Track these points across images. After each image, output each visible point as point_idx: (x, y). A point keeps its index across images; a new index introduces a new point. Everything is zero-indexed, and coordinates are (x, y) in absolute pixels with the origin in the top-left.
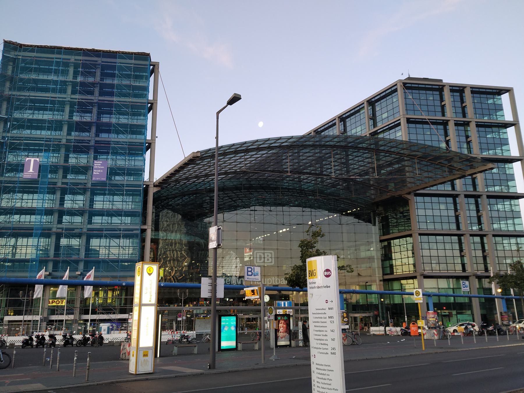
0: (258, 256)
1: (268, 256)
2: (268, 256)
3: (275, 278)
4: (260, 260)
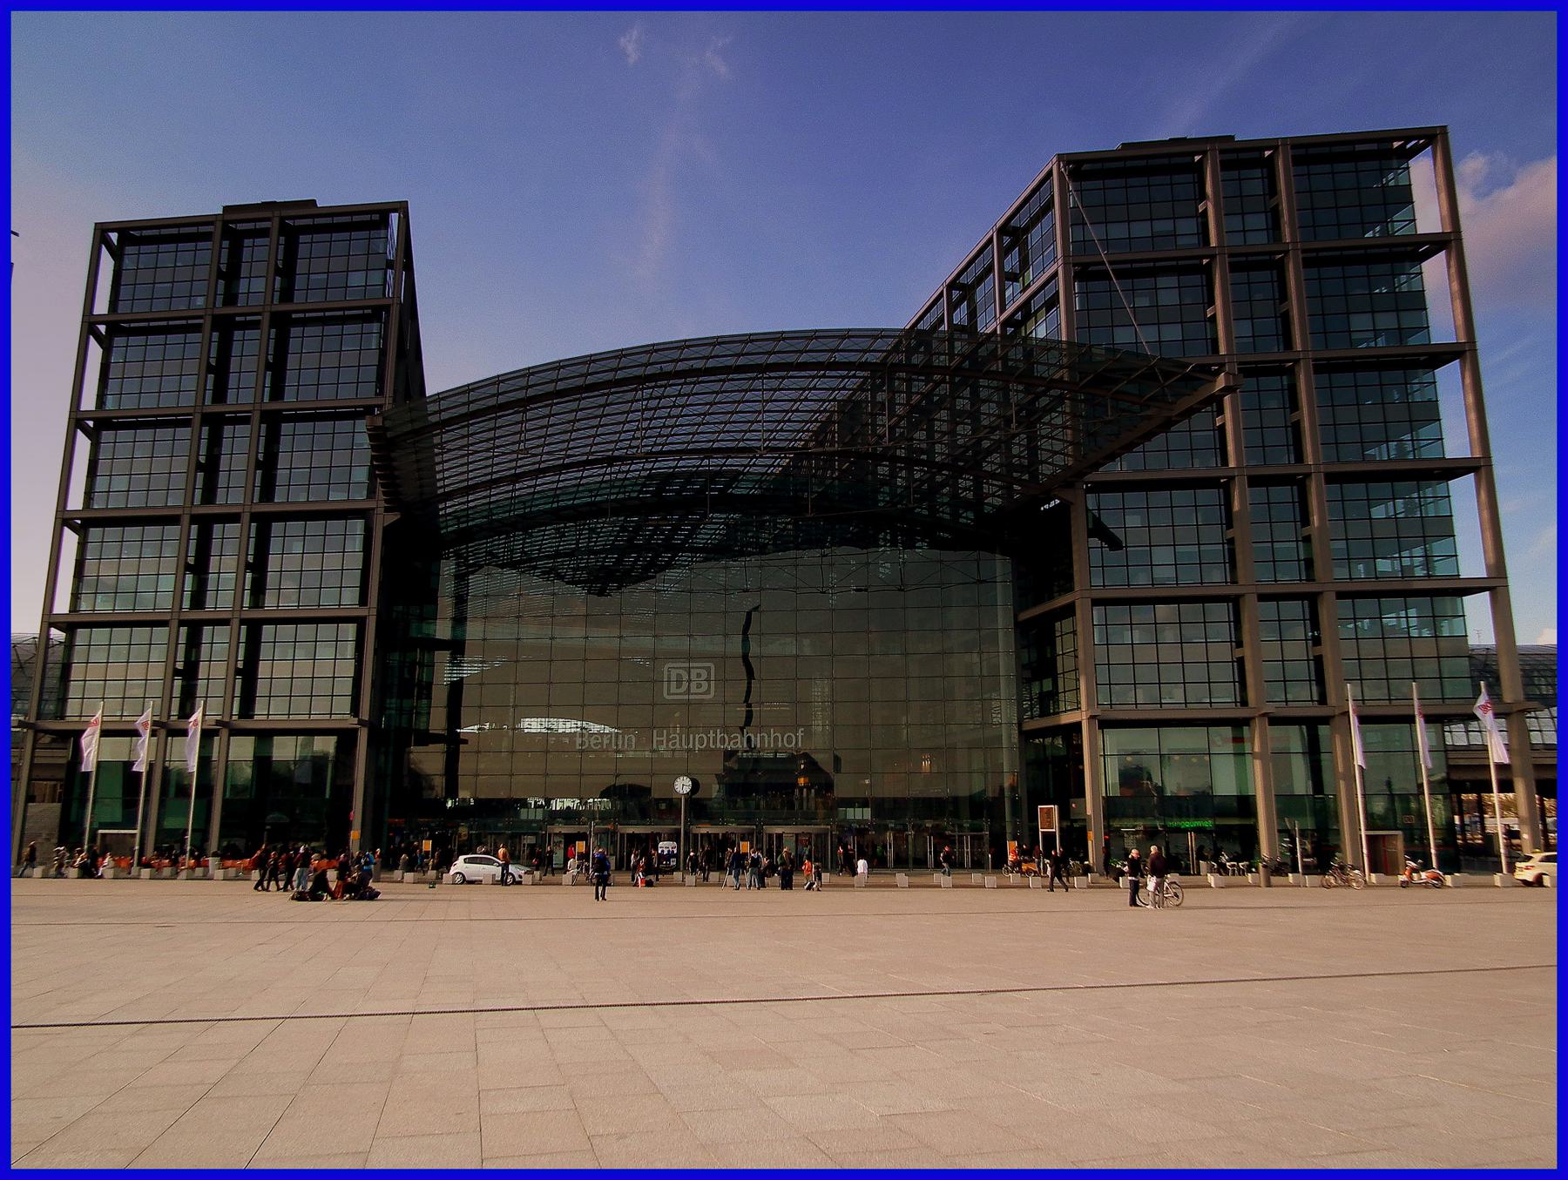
0: (673, 678)
1: (699, 675)
2: (699, 675)
3: (715, 732)
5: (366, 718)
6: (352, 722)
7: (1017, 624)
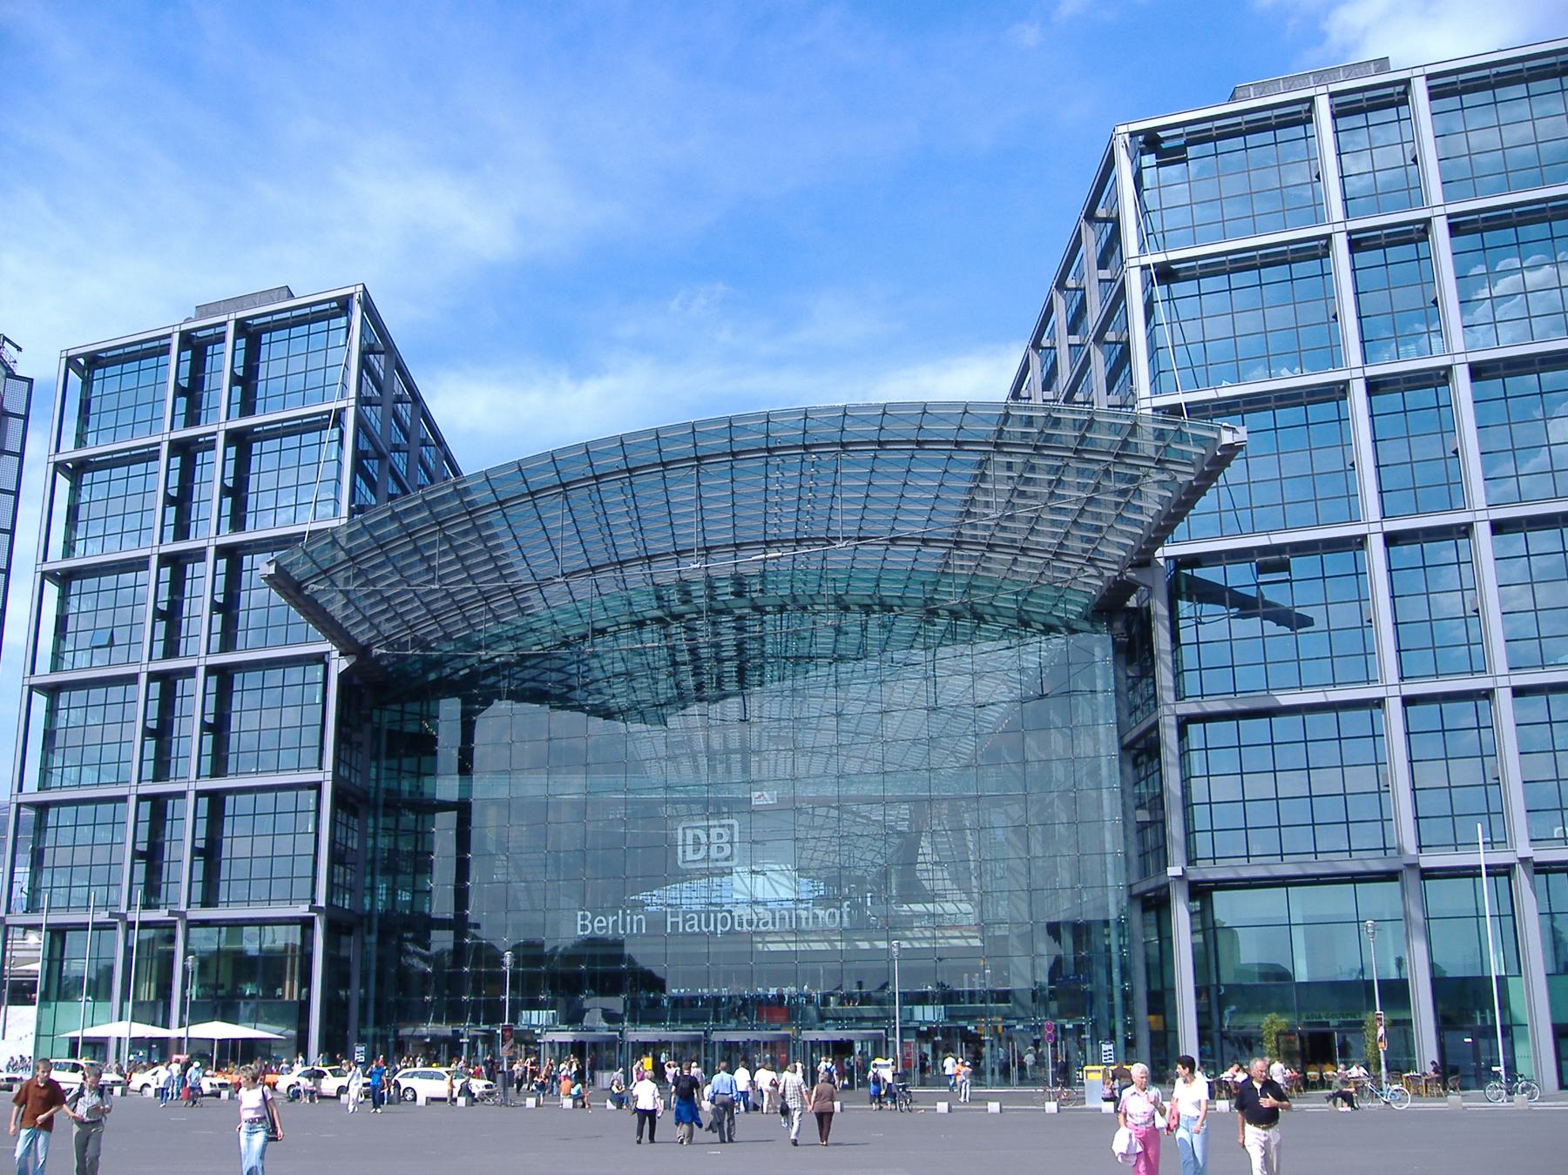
0: (690, 840)
1: (720, 836)
2: (720, 836)
4: (696, 851)
5: (321, 902)
6: (302, 910)
7: (1125, 748)
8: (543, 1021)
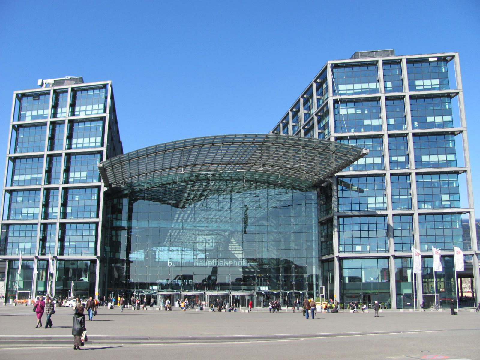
3: (215, 261)
5: (99, 255)
6: (94, 257)
7: (319, 222)
8: (156, 289)
